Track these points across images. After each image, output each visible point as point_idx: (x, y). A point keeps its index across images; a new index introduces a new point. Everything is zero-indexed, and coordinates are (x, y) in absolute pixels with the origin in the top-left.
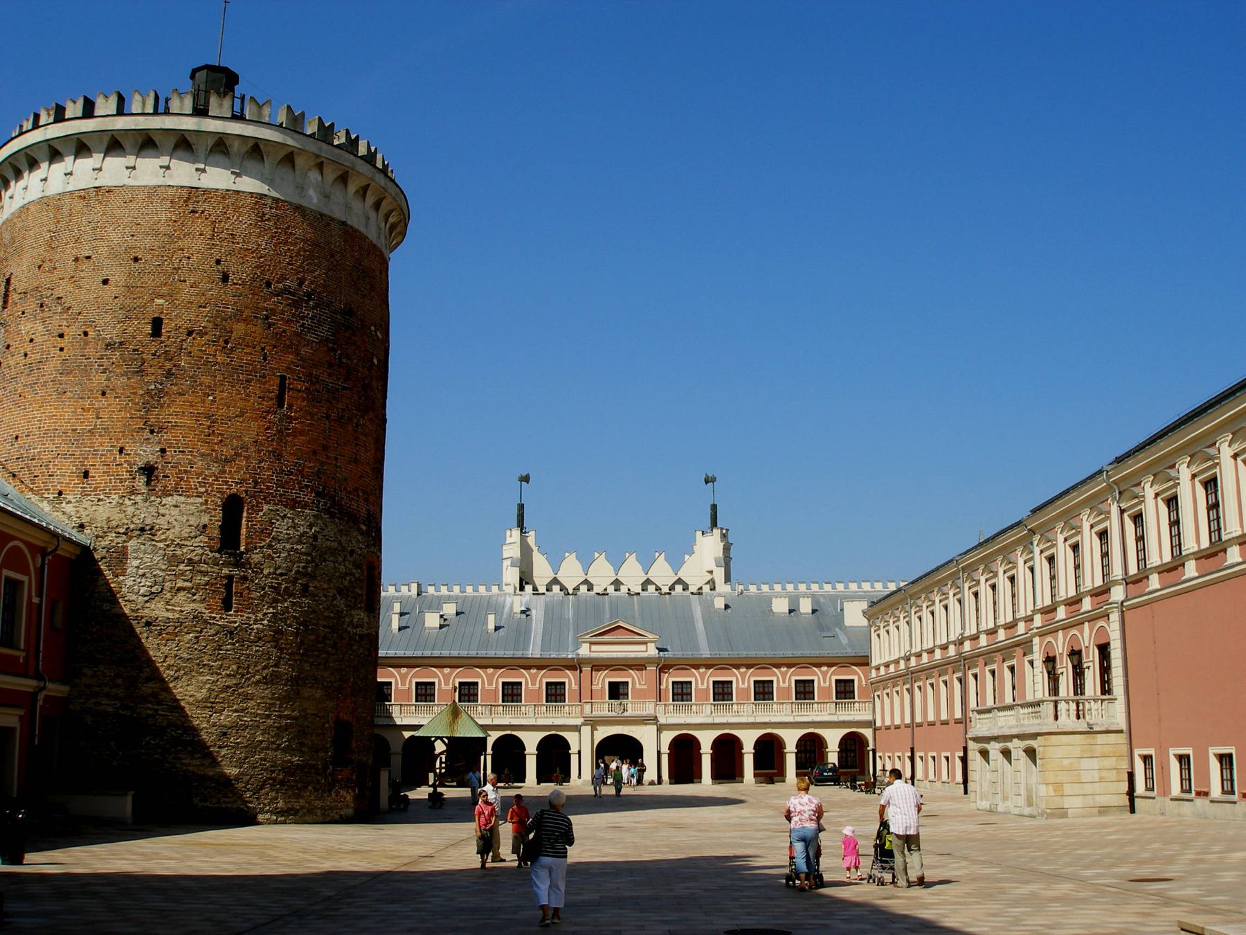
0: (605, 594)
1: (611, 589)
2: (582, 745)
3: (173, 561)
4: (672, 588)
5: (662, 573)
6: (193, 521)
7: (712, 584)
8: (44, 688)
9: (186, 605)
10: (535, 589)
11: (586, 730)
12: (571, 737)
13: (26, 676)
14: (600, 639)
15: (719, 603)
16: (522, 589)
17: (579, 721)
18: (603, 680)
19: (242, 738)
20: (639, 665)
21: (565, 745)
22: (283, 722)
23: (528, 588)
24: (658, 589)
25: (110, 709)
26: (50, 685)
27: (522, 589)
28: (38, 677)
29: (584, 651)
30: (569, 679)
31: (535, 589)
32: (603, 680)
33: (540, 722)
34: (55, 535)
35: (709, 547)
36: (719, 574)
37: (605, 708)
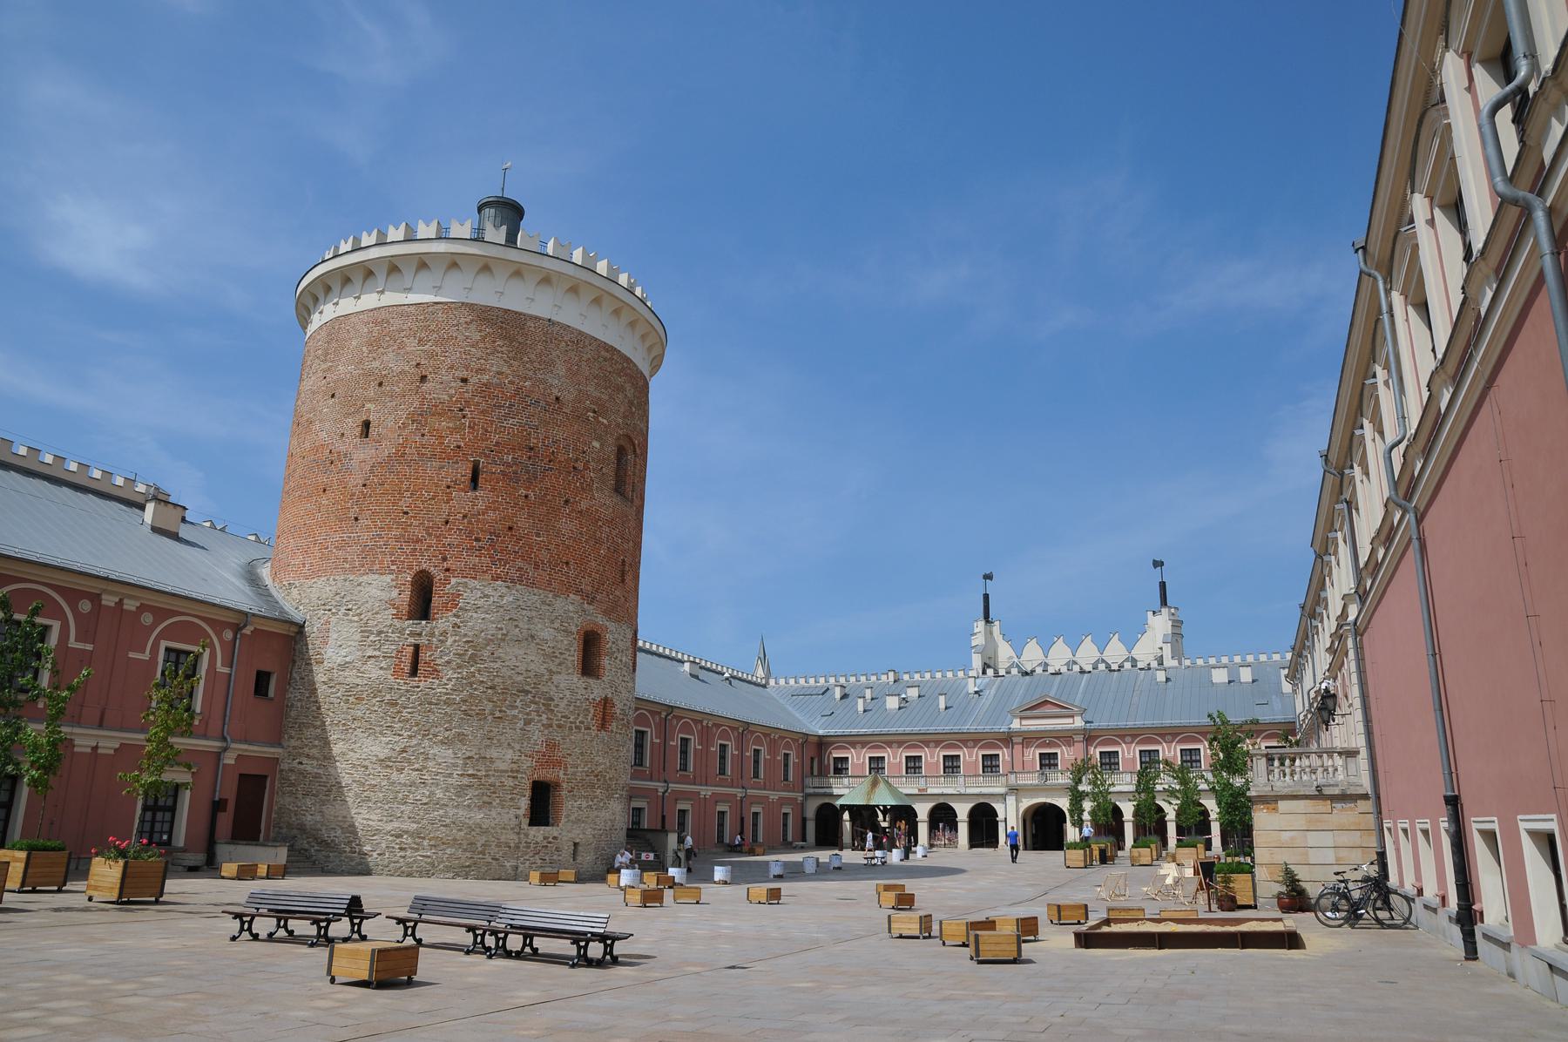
0: (1058, 673)
1: (1064, 669)
2: (1010, 815)
3: (366, 633)
4: (1121, 666)
5: (1115, 652)
6: (384, 596)
7: (1160, 661)
8: (225, 749)
9: (374, 672)
10: (996, 672)
11: (1011, 800)
12: (999, 807)
13: (205, 736)
14: (1028, 713)
15: (1161, 676)
16: (984, 672)
17: (1002, 790)
18: (1033, 754)
19: (421, 794)
20: (1066, 738)
21: (994, 813)
22: (466, 781)
23: (990, 672)
24: (1108, 667)
25: (309, 768)
26: (233, 746)
27: (984, 672)
28: (224, 739)
29: (1016, 725)
30: (1004, 754)
31: (996, 672)
32: (1033, 754)
33: (970, 791)
34: (246, 614)
35: (1160, 625)
36: (1167, 649)
37: (1031, 779)
